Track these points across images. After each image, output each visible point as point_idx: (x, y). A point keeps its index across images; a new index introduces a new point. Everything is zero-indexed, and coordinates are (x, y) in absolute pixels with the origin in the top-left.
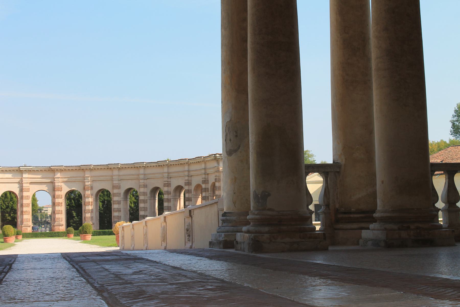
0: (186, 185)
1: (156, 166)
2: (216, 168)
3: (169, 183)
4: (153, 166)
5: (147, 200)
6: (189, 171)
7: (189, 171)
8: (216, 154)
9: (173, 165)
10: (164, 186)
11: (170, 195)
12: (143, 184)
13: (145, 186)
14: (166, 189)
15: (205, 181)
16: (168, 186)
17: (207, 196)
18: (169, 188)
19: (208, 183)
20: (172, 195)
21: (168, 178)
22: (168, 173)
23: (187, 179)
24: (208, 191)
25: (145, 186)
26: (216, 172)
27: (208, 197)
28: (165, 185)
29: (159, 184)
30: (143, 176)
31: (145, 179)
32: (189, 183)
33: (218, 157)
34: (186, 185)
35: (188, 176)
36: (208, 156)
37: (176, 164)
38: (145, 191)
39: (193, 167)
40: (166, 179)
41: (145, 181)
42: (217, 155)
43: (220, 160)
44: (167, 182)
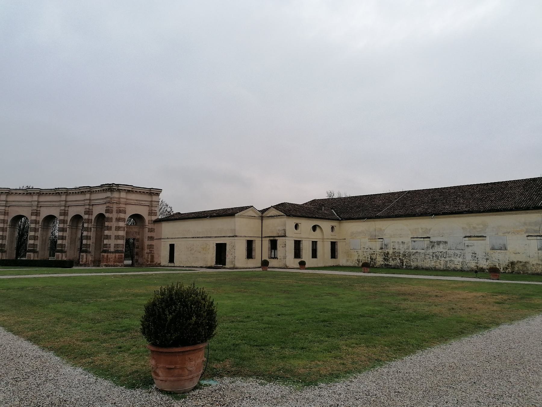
0: (60, 215)
1: (24, 193)
2: (109, 199)
3: (39, 212)
4: (20, 193)
5: (7, 228)
6: (66, 201)
7: (66, 201)
8: (113, 184)
9: (47, 193)
10: (32, 215)
11: (37, 225)
12: (4, 211)
13: (6, 213)
14: (34, 218)
15: (89, 212)
16: (36, 215)
17: (90, 227)
18: (38, 217)
19: (92, 215)
20: (40, 224)
21: (37, 207)
22: (38, 202)
23: (63, 209)
24: (91, 223)
25: (6, 213)
26: (109, 202)
27: (91, 228)
28: (32, 214)
29: (25, 212)
30: (5, 203)
31: (6, 206)
32: (65, 214)
33: (114, 187)
34: (60, 215)
35: (65, 206)
36: (100, 186)
37: (50, 193)
38: (6, 219)
39: (70, 198)
40: (35, 208)
41: (7, 208)
42: (114, 185)
43: (115, 190)
44: (35, 211)
